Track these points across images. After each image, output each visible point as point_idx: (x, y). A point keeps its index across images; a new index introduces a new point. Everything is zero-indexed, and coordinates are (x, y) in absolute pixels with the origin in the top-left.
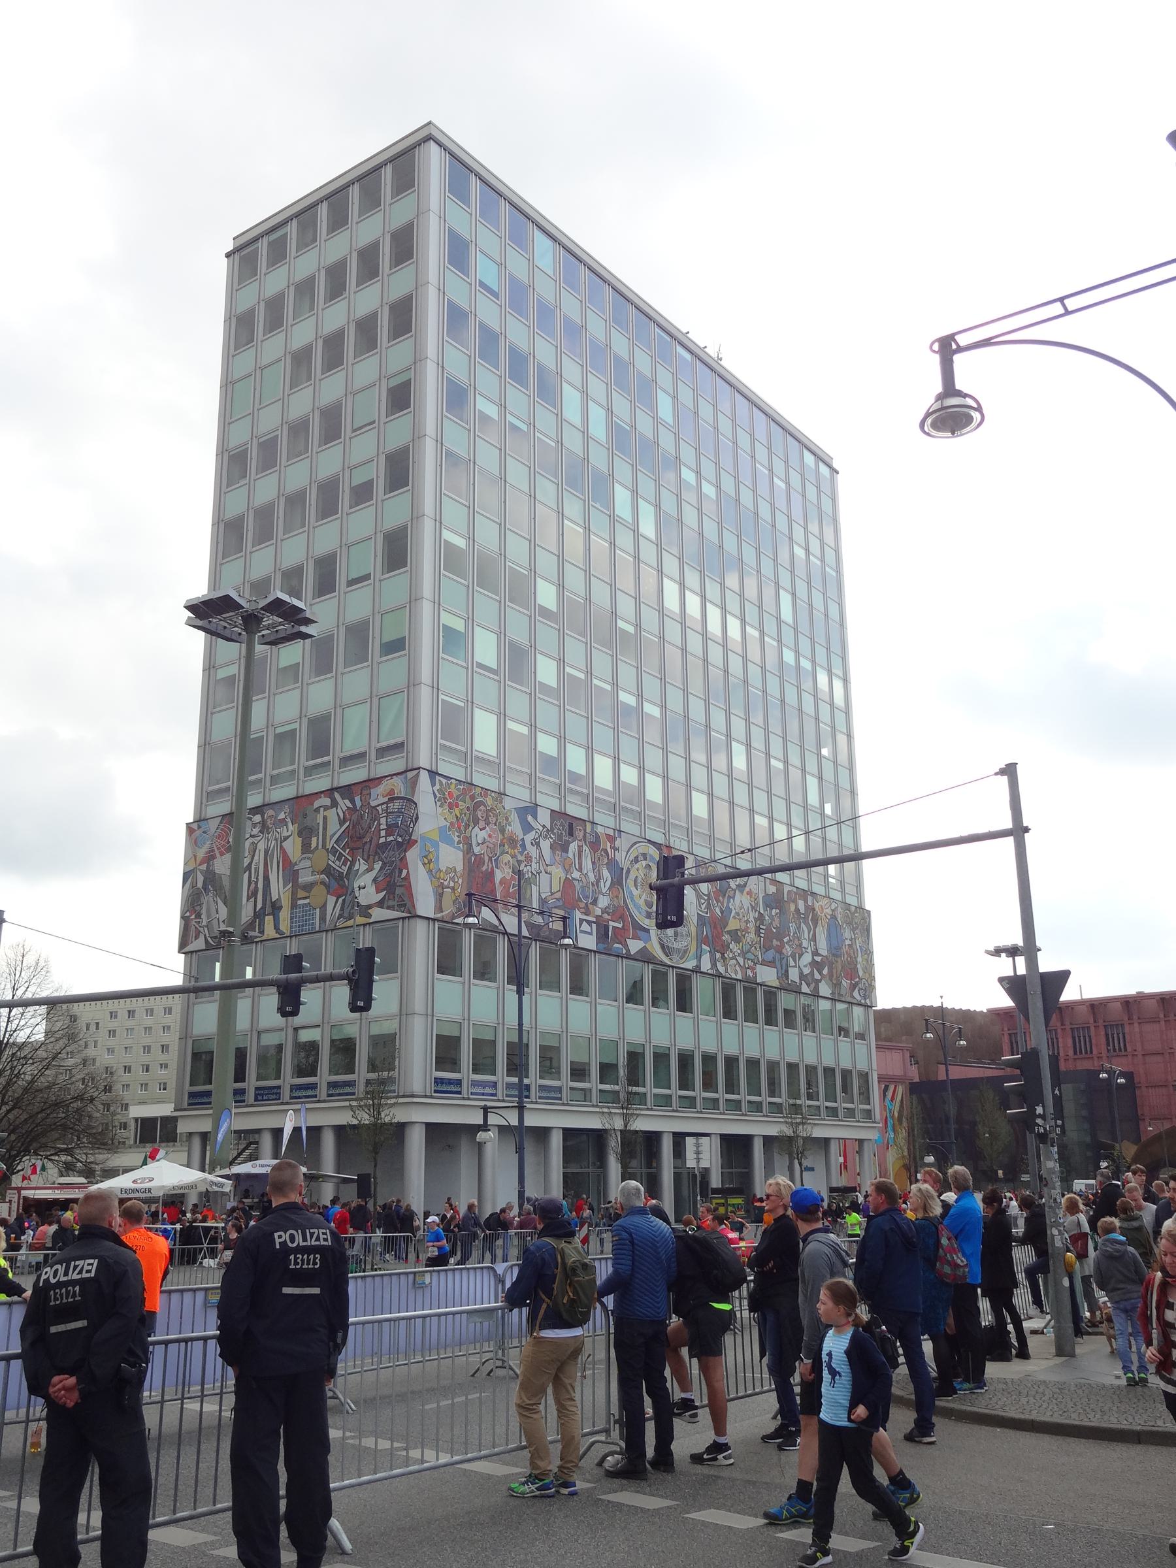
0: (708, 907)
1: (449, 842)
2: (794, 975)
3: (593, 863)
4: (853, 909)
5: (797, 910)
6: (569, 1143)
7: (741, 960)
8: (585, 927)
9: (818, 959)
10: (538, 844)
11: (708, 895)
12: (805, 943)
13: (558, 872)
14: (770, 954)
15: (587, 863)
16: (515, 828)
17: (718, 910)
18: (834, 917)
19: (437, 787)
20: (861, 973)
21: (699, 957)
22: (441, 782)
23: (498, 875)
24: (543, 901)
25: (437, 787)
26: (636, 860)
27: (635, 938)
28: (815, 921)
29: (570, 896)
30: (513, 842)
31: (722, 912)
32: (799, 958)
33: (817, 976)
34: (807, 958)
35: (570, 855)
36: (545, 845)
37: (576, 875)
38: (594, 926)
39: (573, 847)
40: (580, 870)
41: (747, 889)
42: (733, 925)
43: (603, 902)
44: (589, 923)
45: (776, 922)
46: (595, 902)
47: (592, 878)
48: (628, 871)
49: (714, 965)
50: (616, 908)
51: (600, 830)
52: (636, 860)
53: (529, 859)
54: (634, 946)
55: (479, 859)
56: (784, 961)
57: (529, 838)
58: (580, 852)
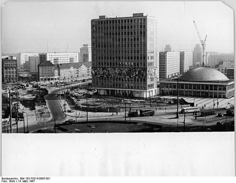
2: (132, 76)
5: (133, 71)
11: (120, 71)
13: (103, 72)
15: (105, 71)
16: (99, 70)
18: (140, 70)
20: (144, 75)
21: (118, 76)
28: (136, 71)
29: (104, 74)
34: (135, 75)
36: (101, 71)
42: (123, 73)
43: (107, 73)
49: (120, 76)
54: (110, 76)
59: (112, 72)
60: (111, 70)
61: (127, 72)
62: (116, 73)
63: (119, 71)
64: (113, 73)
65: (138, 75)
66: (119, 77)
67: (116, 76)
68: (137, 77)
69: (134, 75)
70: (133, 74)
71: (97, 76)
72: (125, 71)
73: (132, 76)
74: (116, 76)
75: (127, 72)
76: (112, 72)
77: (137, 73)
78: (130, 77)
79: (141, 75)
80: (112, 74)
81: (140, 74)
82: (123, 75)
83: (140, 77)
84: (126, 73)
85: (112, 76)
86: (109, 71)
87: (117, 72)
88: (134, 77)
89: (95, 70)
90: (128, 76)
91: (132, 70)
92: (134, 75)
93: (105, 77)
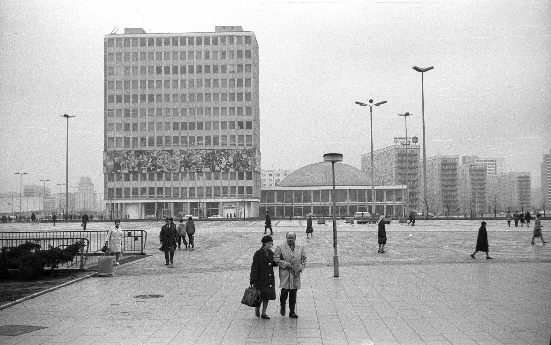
0: (184, 159)
1: (110, 161)
2: (217, 168)
3: (147, 158)
4: (247, 150)
6: (293, 192)
7: (196, 168)
8: (144, 169)
9: (229, 164)
10: (131, 157)
11: (185, 157)
12: (223, 161)
13: (138, 161)
14: (208, 165)
15: (145, 158)
16: (126, 155)
17: (188, 160)
18: (238, 153)
19: (107, 153)
20: (249, 164)
21: (180, 170)
22: (108, 153)
23: (121, 164)
24: (132, 167)
25: (107, 153)
26: (160, 154)
27: (159, 169)
28: (228, 156)
29: (140, 165)
30: (124, 158)
31: (189, 159)
32: (220, 165)
33: (228, 167)
34: (225, 164)
35: (140, 157)
36: (133, 157)
37: (142, 160)
38: (147, 169)
39: (141, 156)
40: (143, 159)
41: (200, 153)
44: (145, 168)
45: (211, 158)
46: (147, 164)
47: (146, 160)
48: (157, 157)
49: (185, 170)
50: (153, 165)
51: (148, 151)
52: (160, 154)
53: (129, 160)
54: (158, 170)
55: (117, 162)
56: (214, 167)
57: (128, 157)
58: (143, 156)
59: (163, 159)
60: (161, 156)
61: (205, 158)
62: (174, 162)
63: (183, 156)
64: (167, 161)
65: (235, 165)
66: (183, 170)
67: (175, 170)
68: (231, 170)
69: (223, 166)
70: (221, 163)
71: (119, 171)
72: (199, 156)
73: (217, 168)
74: (175, 170)
75: (205, 158)
76: (163, 159)
77: (231, 160)
78: (213, 170)
79: (242, 165)
80: (164, 164)
81: (239, 160)
82: (193, 166)
83: (238, 168)
84: (203, 161)
85: (165, 170)
86: (154, 159)
87: (177, 158)
88: (223, 169)
89: (116, 156)
90: (209, 167)
91: (219, 154)
92: (223, 166)
93: (145, 171)
